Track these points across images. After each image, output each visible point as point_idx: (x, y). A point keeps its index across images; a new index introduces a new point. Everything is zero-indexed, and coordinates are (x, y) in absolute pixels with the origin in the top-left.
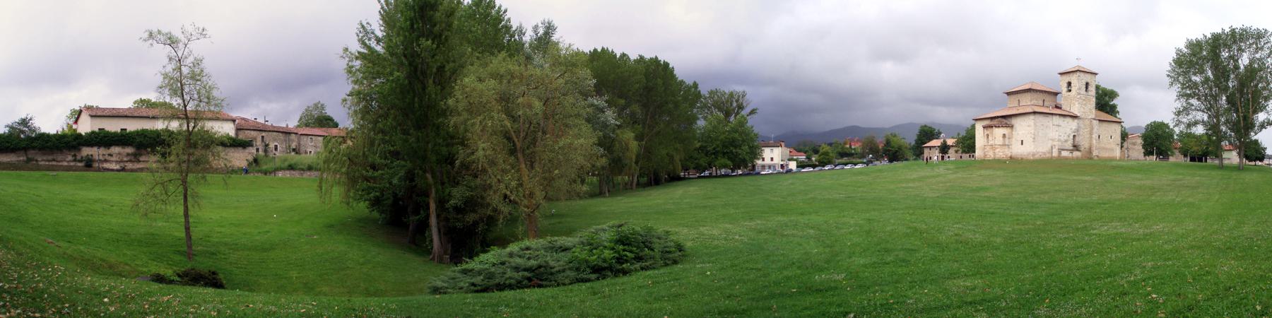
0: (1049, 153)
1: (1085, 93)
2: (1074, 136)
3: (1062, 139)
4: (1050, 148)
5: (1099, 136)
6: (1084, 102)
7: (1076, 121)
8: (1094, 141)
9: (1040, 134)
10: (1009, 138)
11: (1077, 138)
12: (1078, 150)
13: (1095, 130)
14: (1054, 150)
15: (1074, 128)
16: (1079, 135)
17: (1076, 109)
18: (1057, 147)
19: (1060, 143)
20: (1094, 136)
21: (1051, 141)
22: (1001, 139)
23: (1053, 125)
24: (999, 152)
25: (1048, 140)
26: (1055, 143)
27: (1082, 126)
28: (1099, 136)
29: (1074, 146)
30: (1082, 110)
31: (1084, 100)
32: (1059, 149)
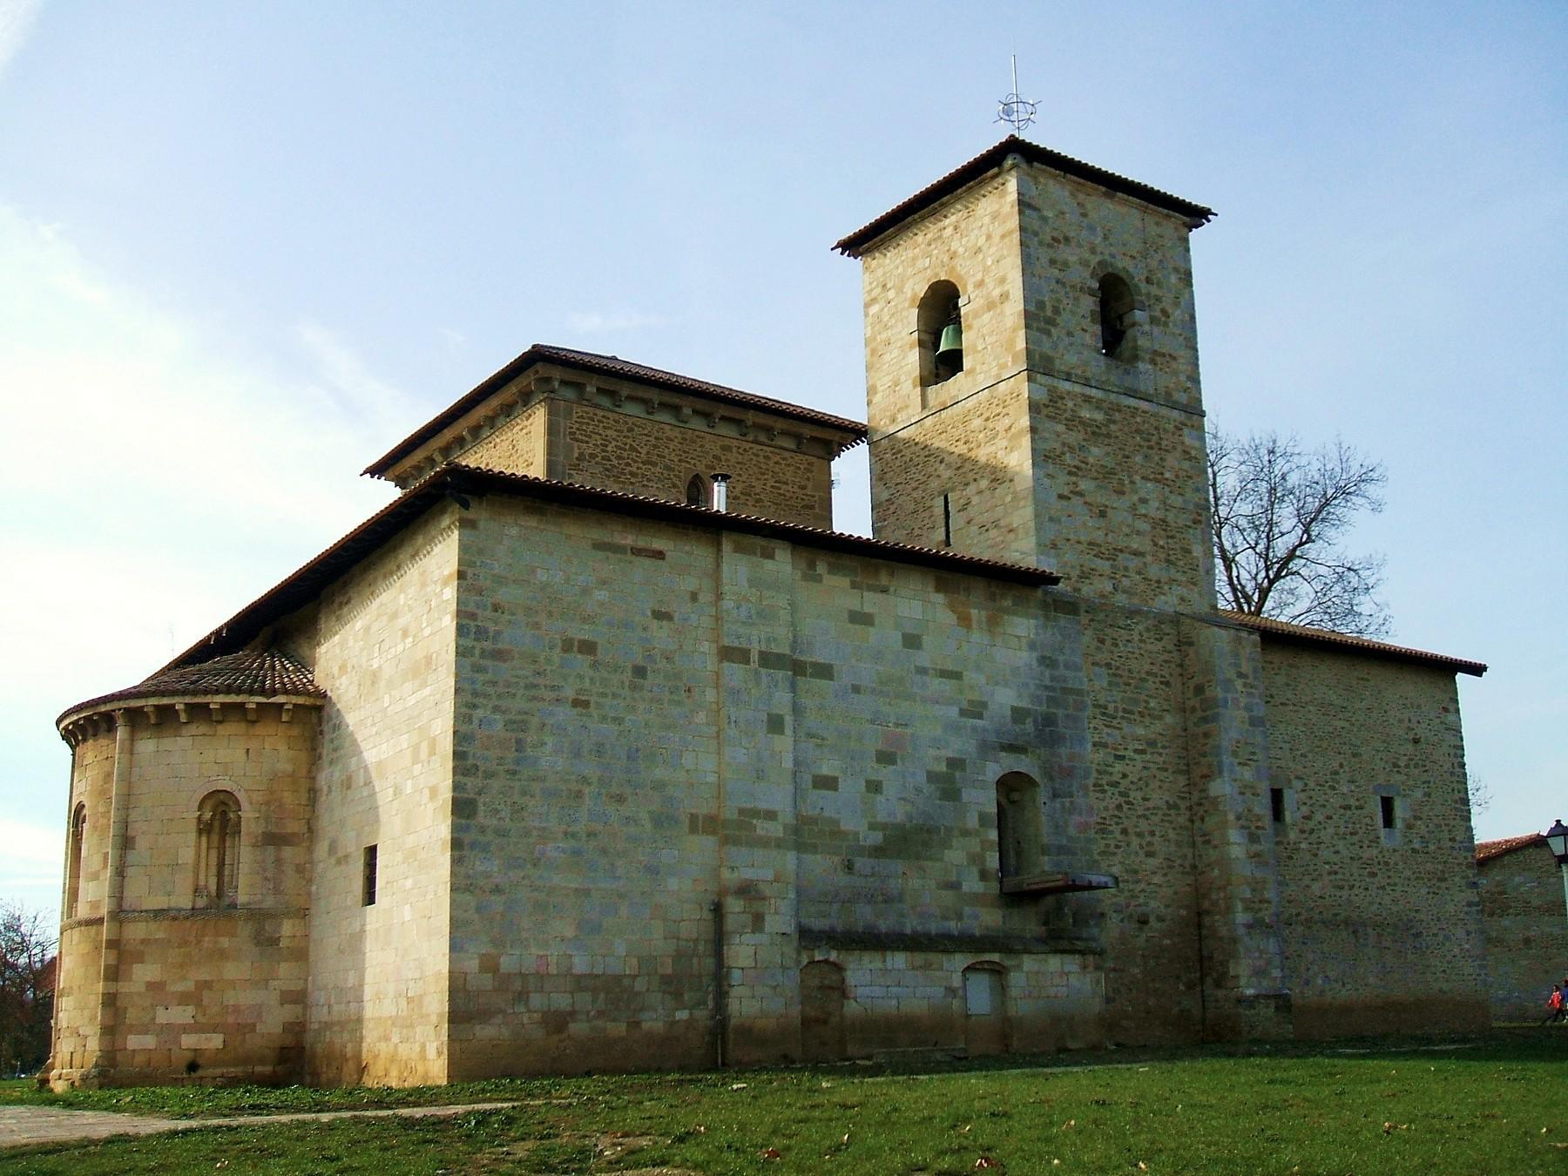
0: (673, 985)
1: (1095, 363)
2: (1012, 787)
3: (854, 824)
4: (693, 923)
5: (1277, 796)
6: (1096, 452)
7: (1023, 626)
8: (1236, 846)
9: (550, 758)
10: (273, 839)
11: (1043, 814)
12: (1057, 940)
13: (1233, 726)
14: (742, 952)
15: (1005, 699)
16: (1062, 777)
17: (1024, 515)
18: (780, 920)
19: (821, 866)
20: (1221, 787)
21: (702, 847)
22: (187, 847)
23: (730, 654)
24: (155, 987)
25: (658, 821)
26: (755, 866)
27: (1094, 683)
28: (1277, 796)
29: (1015, 898)
30: (1085, 526)
31: (1096, 433)
32: (807, 937)
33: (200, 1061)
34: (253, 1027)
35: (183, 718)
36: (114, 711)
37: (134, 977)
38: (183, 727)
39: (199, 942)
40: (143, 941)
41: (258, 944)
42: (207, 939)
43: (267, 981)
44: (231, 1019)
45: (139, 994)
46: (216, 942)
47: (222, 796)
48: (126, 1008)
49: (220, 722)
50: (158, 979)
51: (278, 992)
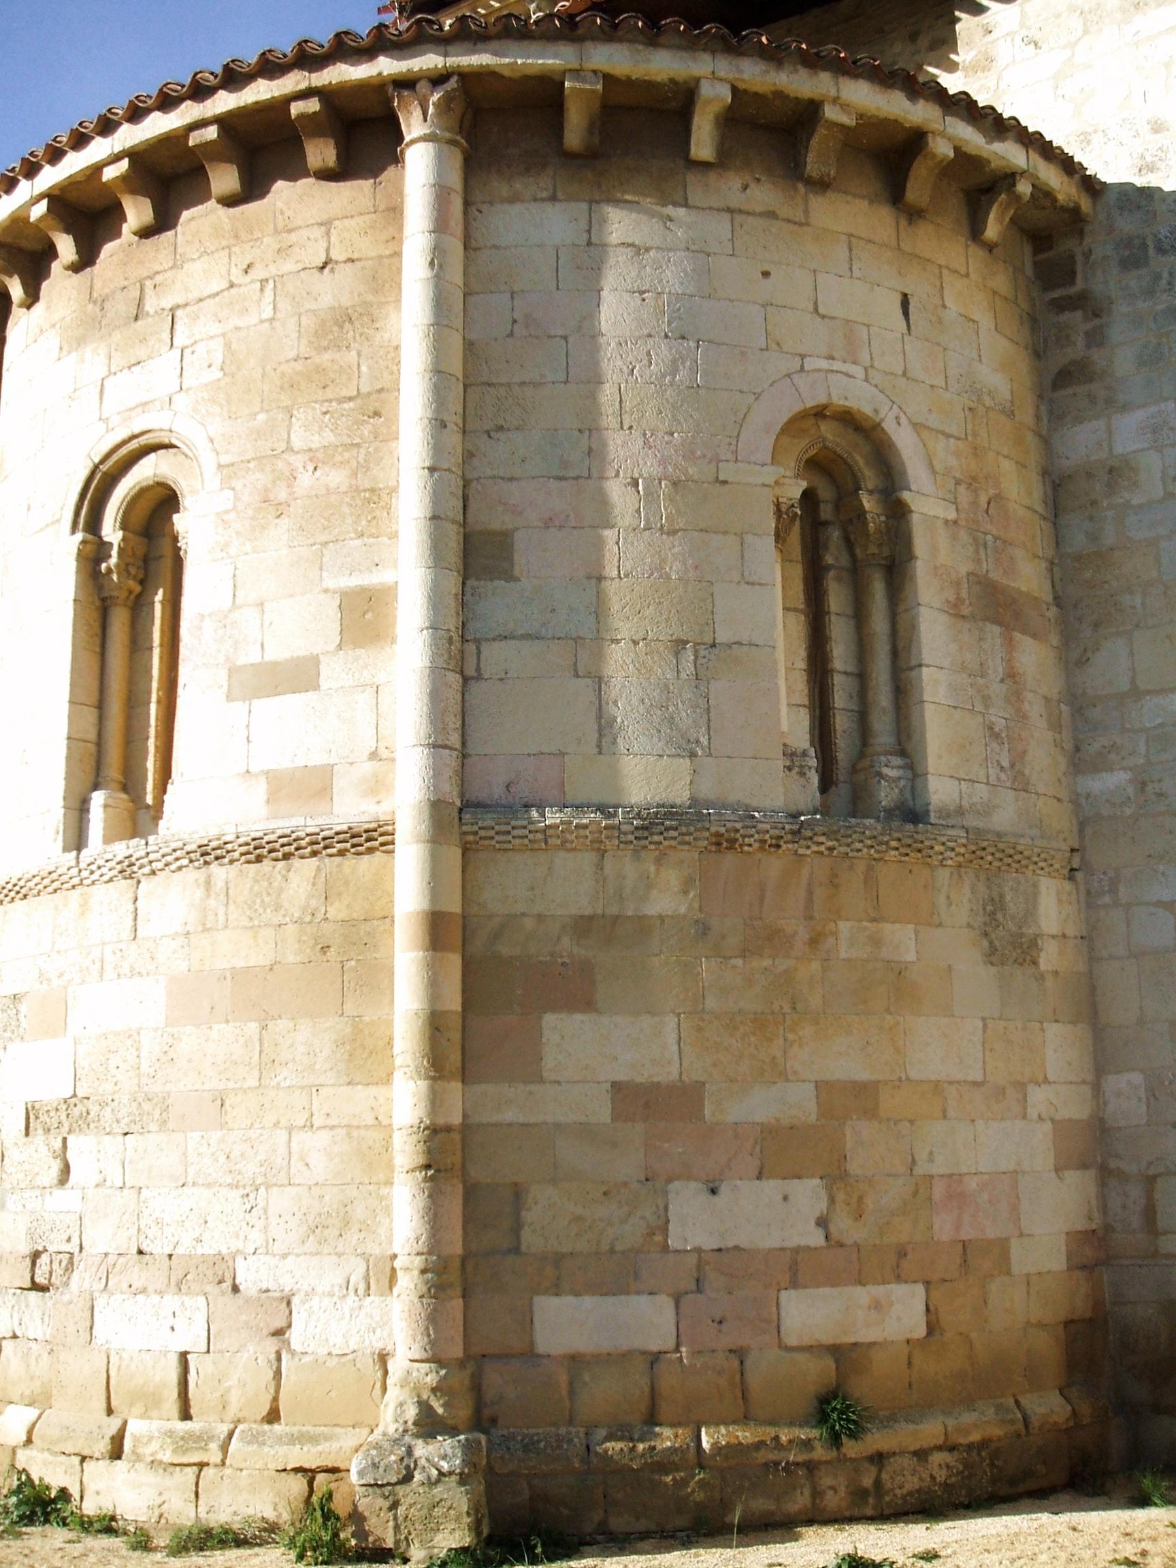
33: (862, 1389)
34: (1001, 1248)
35: (703, 143)
36: (406, 83)
37: (549, 1063)
38: (692, 178)
39: (814, 941)
40: (583, 926)
41: (992, 955)
42: (844, 927)
43: (1021, 1086)
44: (943, 1228)
45: (586, 1132)
46: (876, 941)
47: (828, 431)
48: (518, 1194)
49: (821, 185)
50: (669, 1073)
51: (1048, 1126)
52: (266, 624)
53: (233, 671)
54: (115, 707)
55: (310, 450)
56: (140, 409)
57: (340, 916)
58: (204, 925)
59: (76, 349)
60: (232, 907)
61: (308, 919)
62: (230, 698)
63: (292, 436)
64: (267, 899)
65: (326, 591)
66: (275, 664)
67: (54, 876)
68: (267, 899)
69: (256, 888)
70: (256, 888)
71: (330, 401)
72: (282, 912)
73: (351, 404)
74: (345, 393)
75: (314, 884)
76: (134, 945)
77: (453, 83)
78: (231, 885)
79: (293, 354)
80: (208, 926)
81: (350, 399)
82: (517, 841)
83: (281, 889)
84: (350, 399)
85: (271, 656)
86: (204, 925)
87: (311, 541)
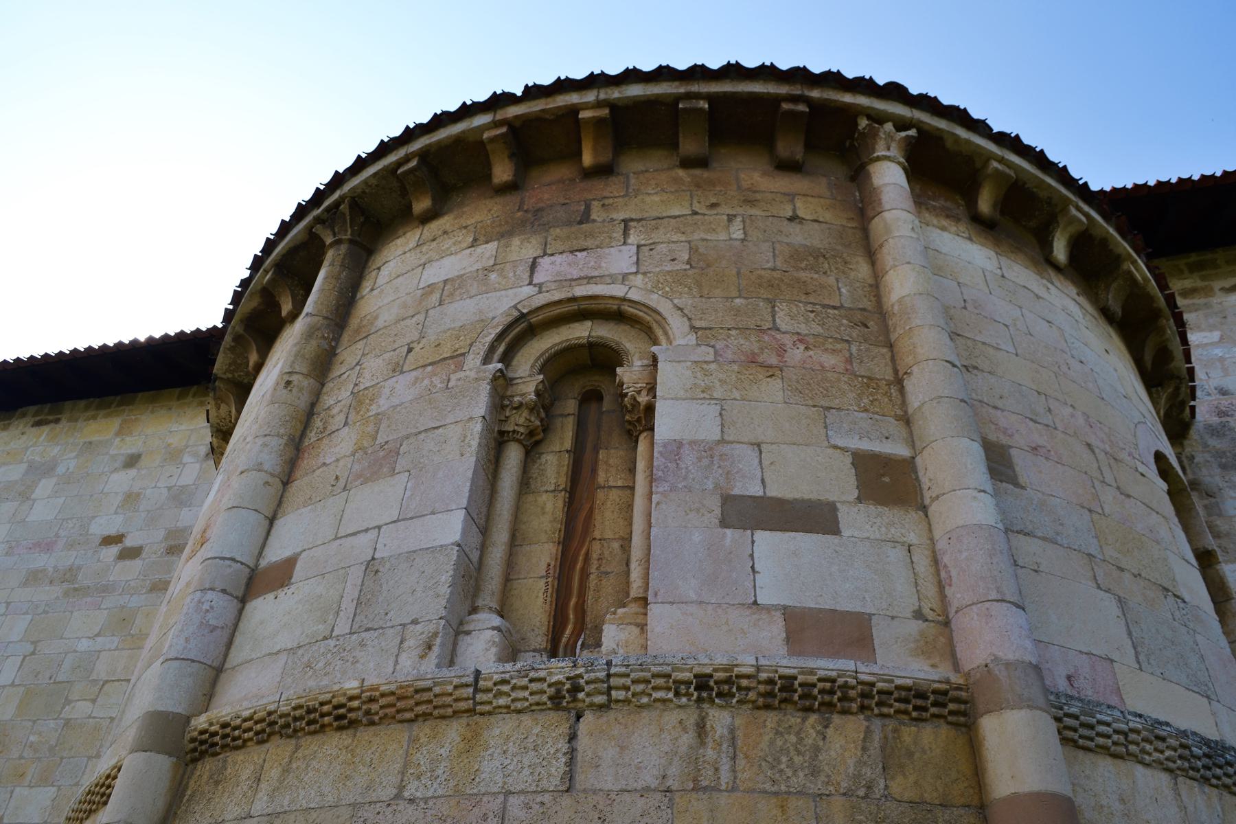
52: (766, 463)
53: (728, 500)
54: (501, 536)
55: (798, 334)
56: (585, 281)
57: (907, 796)
58: (695, 780)
59: (498, 239)
60: (741, 763)
61: (861, 792)
62: (724, 523)
63: (778, 320)
64: (798, 760)
65: (836, 447)
66: (780, 502)
67: (425, 696)
68: (798, 760)
69: (779, 743)
70: (779, 743)
71: (815, 304)
72: (823, 778)
73: (836, 312)
74: (826, 302)
75: (864, 749)
76: (566, 801)
77: (912, 132)
78: (739, 733)
79: (769, 265)
80: (704, 783)
81: (834, 308)
82: (1101, 741)
83: (817, 750)
84: (834, 308)
85: (773, 492)
86: (695, 780)
87: (811, 403)
